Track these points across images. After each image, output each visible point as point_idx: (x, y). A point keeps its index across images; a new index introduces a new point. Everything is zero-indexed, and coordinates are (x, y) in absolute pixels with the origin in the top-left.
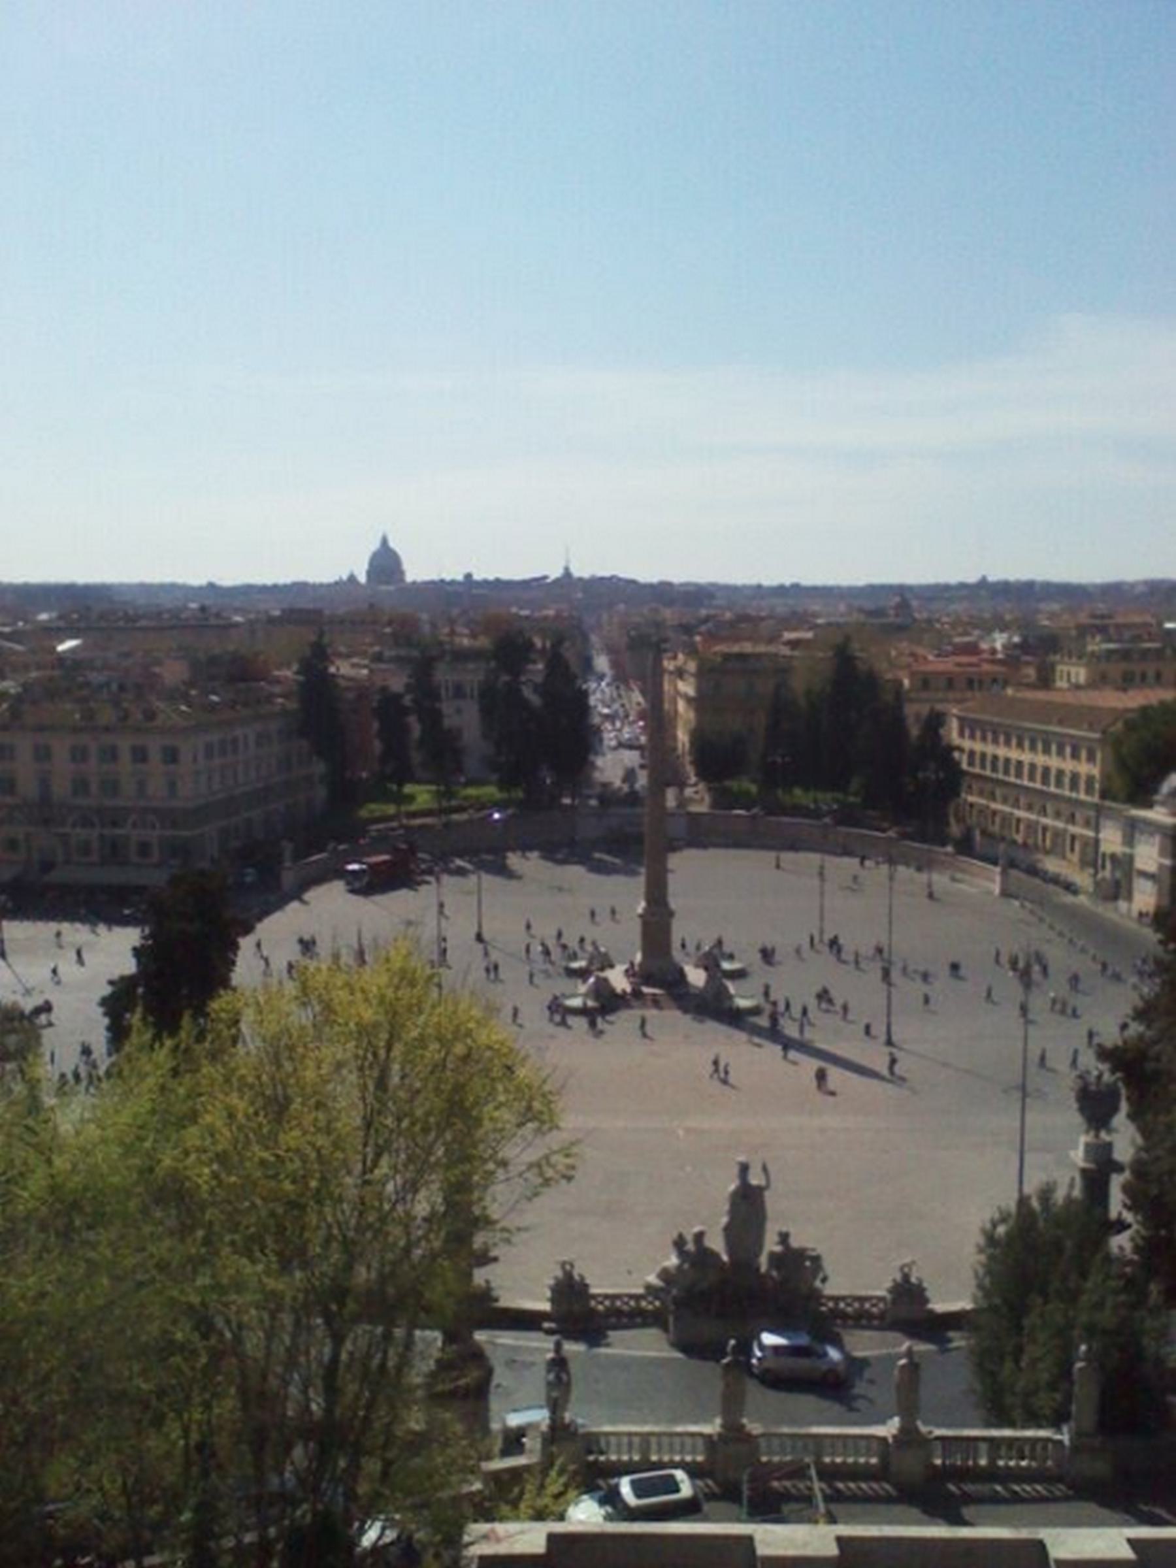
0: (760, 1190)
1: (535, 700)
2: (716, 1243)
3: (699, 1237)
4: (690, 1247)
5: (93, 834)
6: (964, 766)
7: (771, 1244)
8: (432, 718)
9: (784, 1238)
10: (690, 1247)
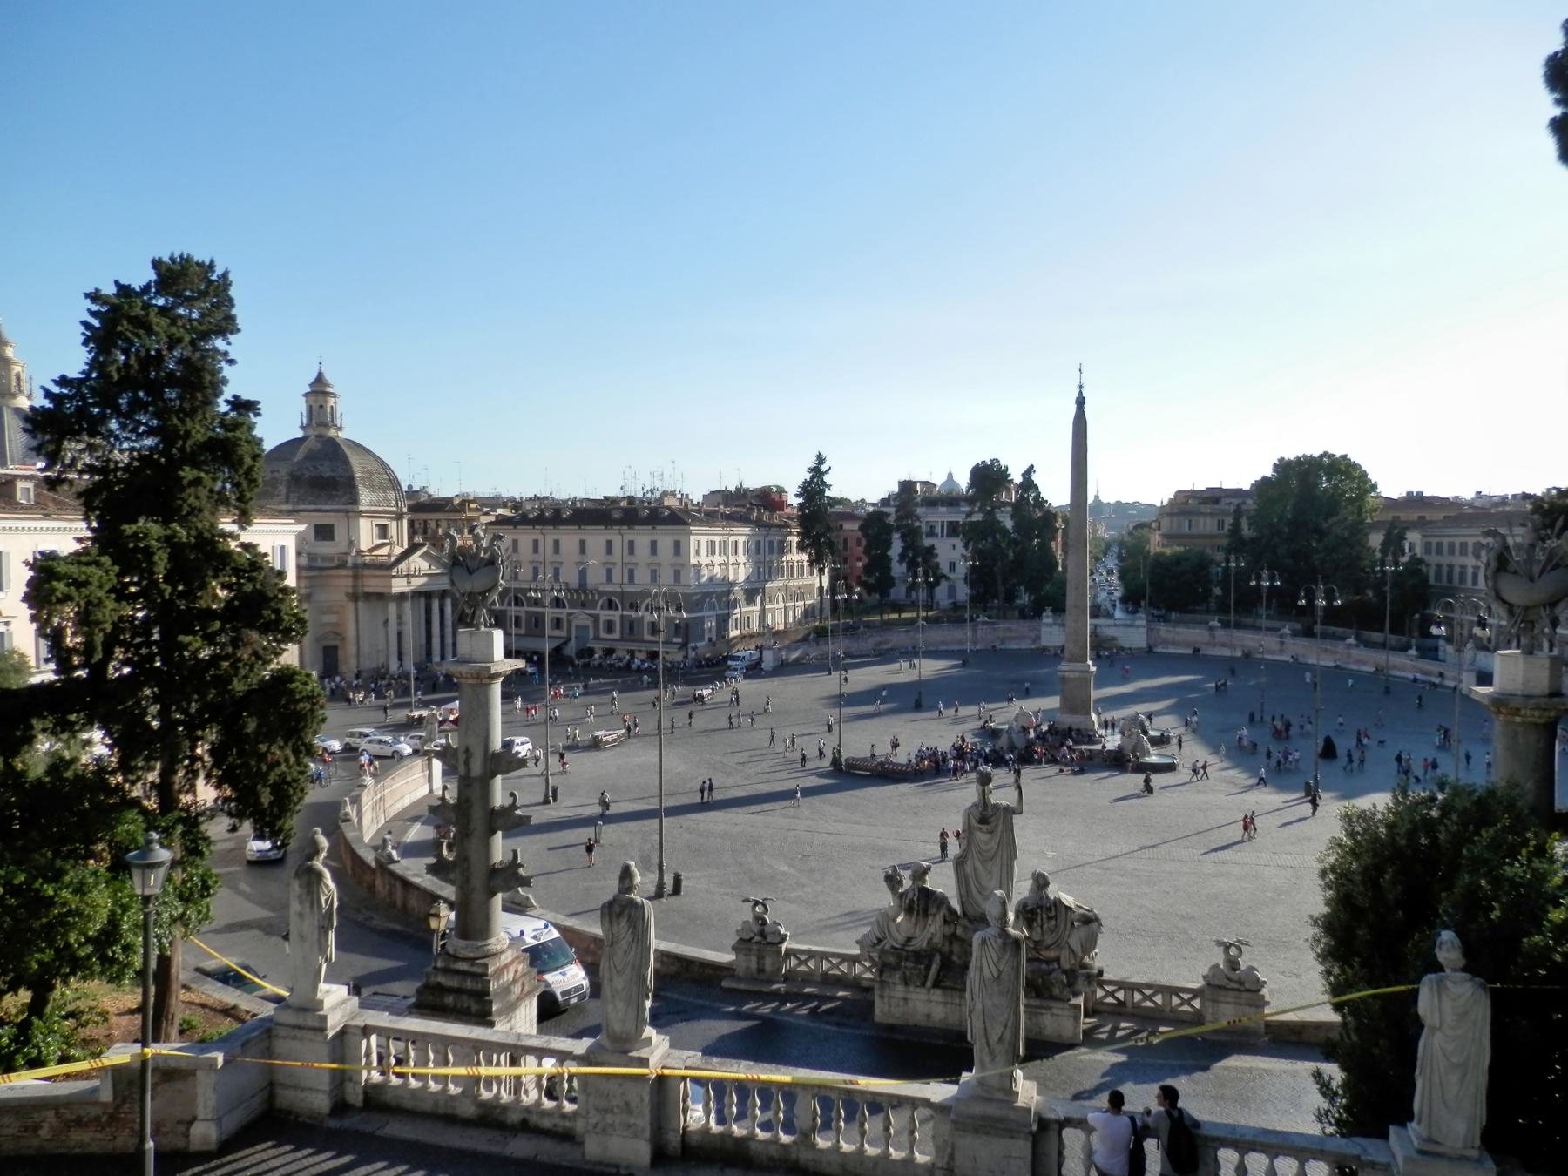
0: (1009, 812)
1: (1009, 524)
2: (942, 881)
3: (920, 874)
4: (907, 883)
5: (615, 615)
6: (1432, 581)
7: (1022, 889)
8: (911, 536)
9: (1041, 882)
10: (907, 883)
